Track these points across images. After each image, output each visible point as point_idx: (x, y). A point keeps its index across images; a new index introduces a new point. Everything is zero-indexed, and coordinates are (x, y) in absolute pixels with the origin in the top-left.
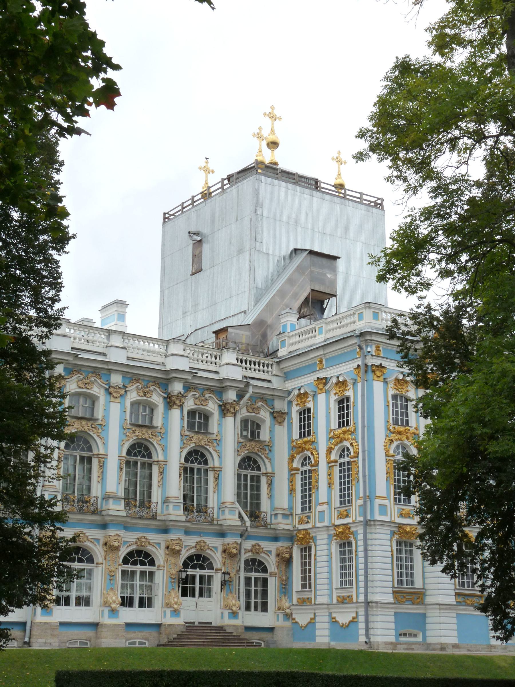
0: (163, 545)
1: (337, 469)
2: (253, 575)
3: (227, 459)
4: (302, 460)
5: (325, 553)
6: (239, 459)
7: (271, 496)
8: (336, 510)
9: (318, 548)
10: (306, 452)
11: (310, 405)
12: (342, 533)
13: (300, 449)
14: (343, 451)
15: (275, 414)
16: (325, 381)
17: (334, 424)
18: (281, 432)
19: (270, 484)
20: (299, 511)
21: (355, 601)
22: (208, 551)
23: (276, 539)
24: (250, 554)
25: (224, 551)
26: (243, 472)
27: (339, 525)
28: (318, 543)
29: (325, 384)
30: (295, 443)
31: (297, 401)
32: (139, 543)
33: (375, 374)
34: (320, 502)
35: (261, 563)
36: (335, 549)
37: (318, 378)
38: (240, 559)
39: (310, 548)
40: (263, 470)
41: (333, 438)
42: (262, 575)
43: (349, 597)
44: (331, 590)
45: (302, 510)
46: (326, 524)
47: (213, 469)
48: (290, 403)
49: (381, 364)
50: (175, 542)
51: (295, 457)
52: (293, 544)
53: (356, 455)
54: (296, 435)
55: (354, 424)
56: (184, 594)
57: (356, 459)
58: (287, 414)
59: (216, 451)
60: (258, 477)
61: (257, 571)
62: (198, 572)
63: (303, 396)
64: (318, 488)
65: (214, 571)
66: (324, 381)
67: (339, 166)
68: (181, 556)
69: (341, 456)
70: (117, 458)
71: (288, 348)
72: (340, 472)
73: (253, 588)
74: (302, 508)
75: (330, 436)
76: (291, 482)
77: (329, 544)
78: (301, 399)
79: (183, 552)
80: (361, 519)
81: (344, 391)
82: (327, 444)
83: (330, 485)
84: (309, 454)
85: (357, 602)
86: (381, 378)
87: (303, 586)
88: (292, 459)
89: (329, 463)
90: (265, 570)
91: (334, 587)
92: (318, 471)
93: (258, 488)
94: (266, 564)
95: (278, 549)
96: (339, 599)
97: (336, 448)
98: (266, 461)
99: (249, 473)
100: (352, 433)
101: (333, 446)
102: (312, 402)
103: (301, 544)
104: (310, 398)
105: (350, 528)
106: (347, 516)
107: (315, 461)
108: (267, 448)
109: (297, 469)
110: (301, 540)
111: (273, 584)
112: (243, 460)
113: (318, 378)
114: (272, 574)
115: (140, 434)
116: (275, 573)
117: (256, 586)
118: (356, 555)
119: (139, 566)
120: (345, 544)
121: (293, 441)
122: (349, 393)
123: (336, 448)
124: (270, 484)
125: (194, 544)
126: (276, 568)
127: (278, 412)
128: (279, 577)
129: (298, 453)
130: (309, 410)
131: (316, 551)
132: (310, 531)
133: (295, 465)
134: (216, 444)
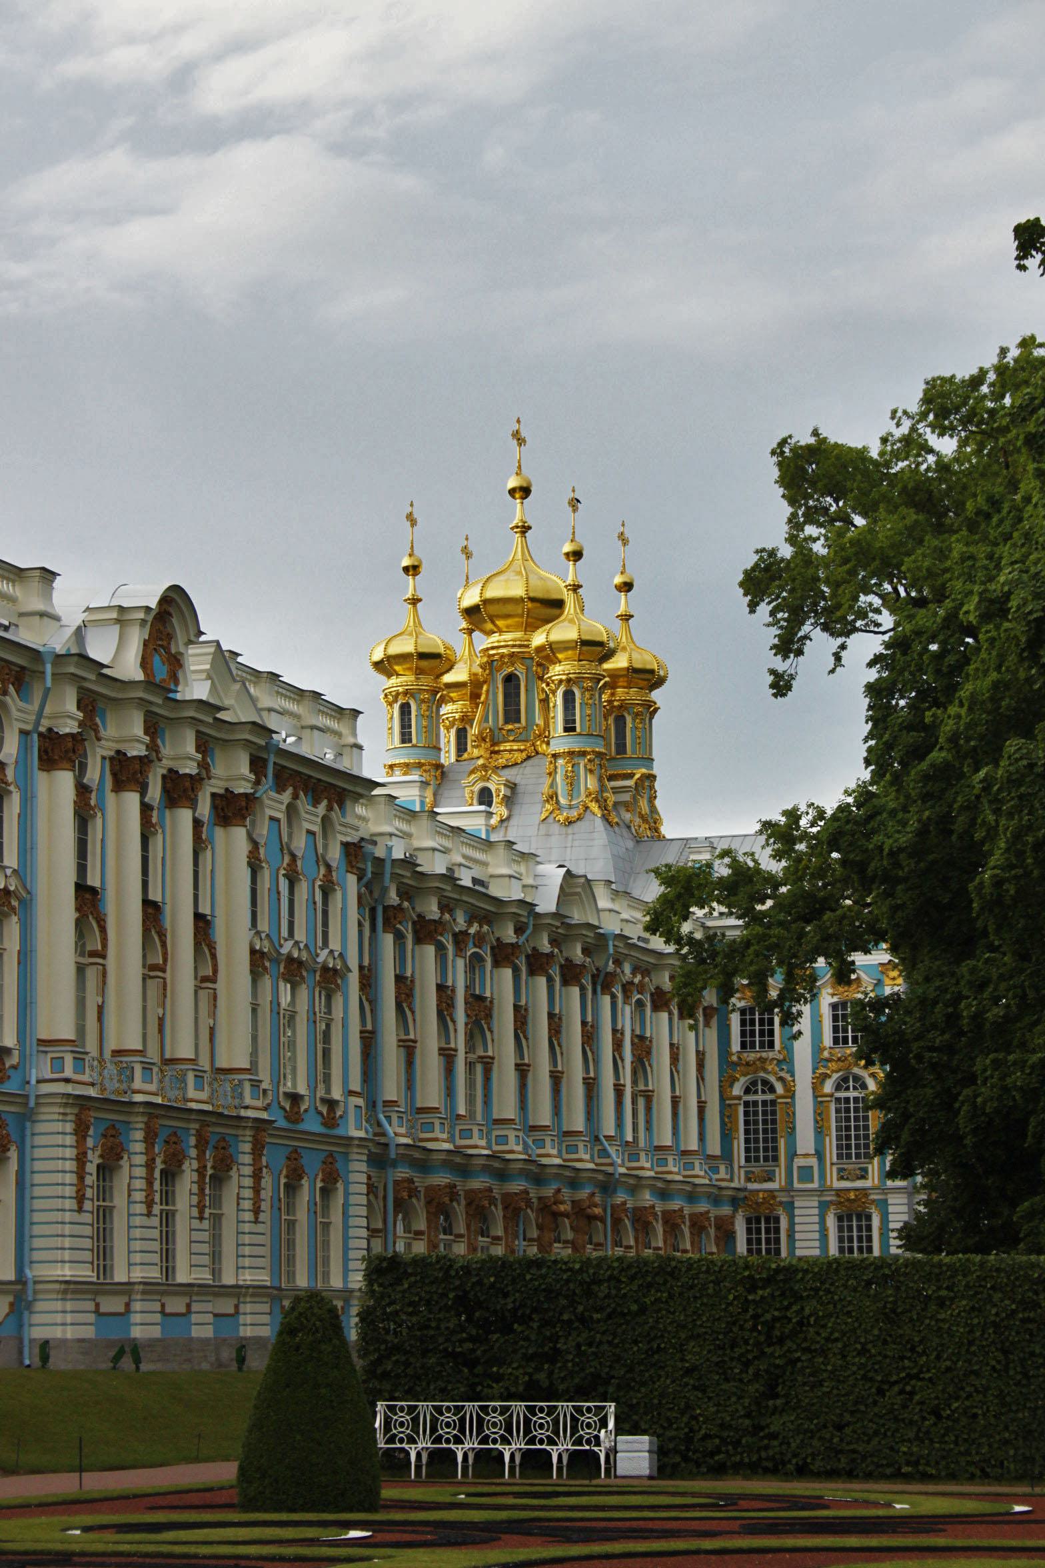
10: (762, 1074)
27: (848, 1190)
28: (797, 1212)
30: (734, 1058)
36: (831, 1222)
45: (748, 1159)
46: (815, 1185)
64: (793, 1129)
84: (772, 1079)
89: (815, 1097)
97: (835, 1076)
109: (739, 1098)
129: (745, 1075)
131: (792, 1224)
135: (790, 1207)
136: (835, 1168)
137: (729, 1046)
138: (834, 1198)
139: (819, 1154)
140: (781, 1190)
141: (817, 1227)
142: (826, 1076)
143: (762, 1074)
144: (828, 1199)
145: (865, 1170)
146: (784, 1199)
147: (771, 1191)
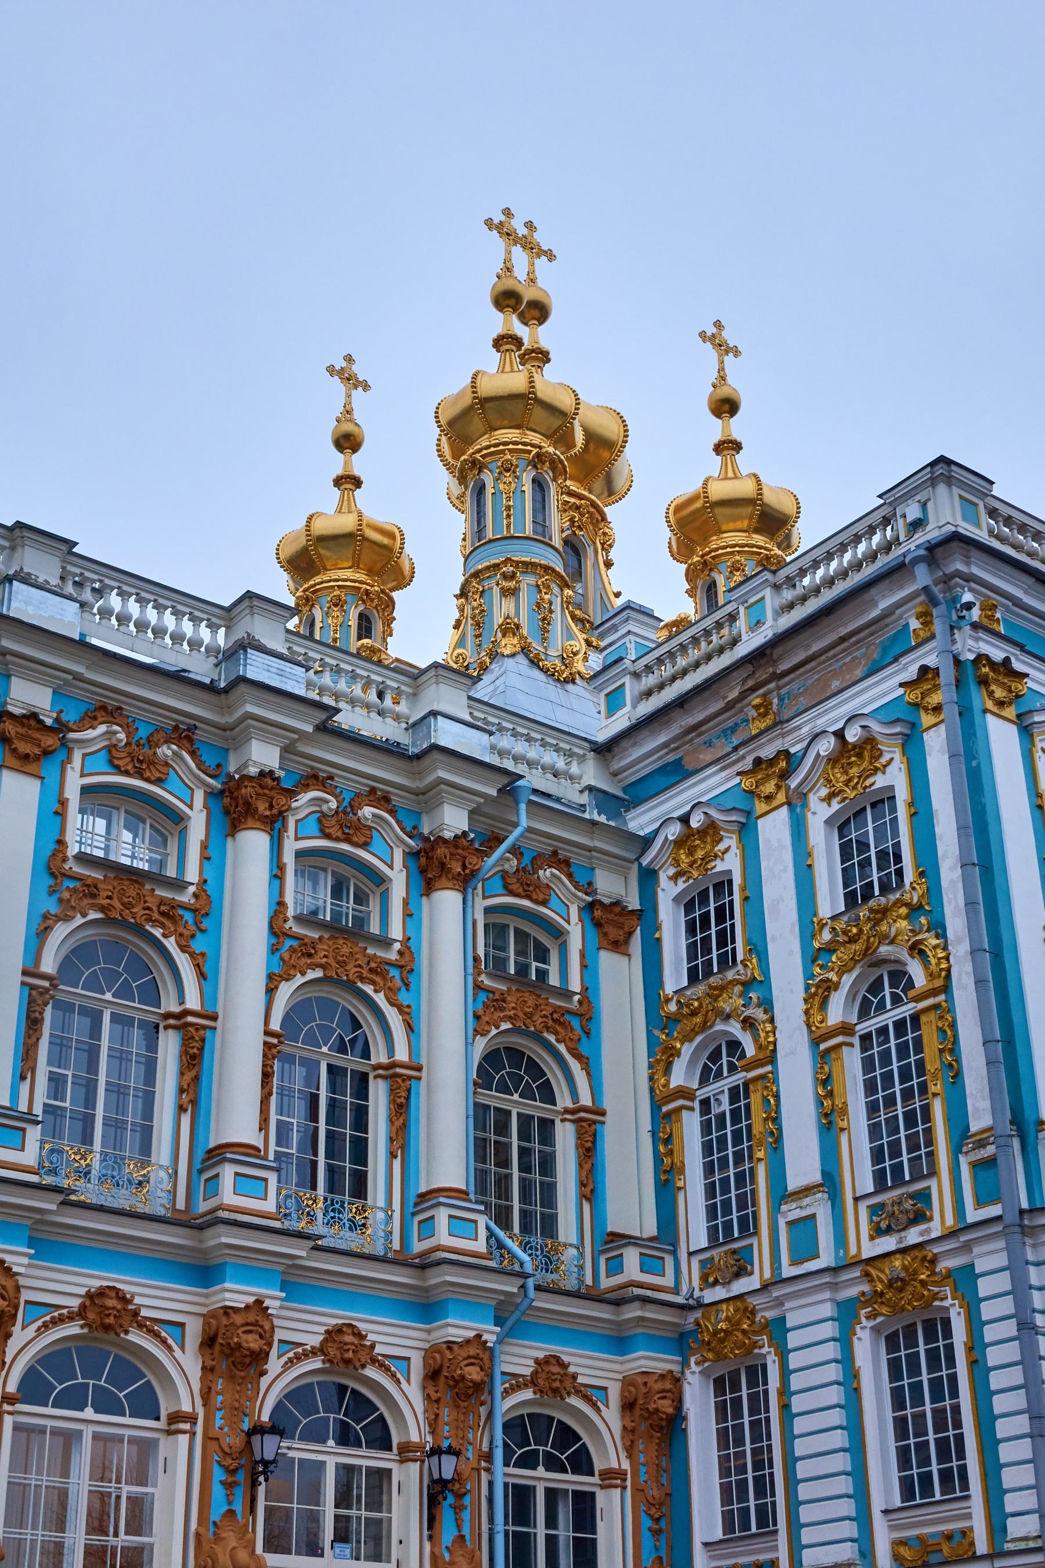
0: (194, 1330)
1: (852, 1059)
2: (541, 1478)
3: (444, 1037)
4: (704, 1059)
5: (828, 1376)
6: (481, 1045)
7: (590, 1189)
8: (863, 1207)
9: (795, 1360)
10: (719, 1027)
11: (731, 863)
12: (898, 1284)
13: (698, 1020)
14: (876, 987)
15: (598, 913)
16: (785, 764)
17: (829, 900)
18: (619, 980)
19: (588, 1149)
20: (701, 1240)
21: (982, 1547)
22: (371, 1372)
23: (619, 1342)
24: (528, 1394)
25: (432, 1375)
26: (494, 1099)
28: (793, 1339)
29: (785, 775)
30: (673, 1007)
31: (677, 862)
32: (91, 1316)
33: (991, 694)
34: (793, 1185)
35: (567, 1436)
36: (868, 1353)
37: (758, 761)
38: (490, 1415)
39: (757, 1373)
40: (564, 1101)
41: (829, 949)
42: (570, 1481)
43: (949, 1537)
44: (863, 1517)
46: (825, 1260)
47: (390, 1071)
48: (648, 877)
49: (1007, 660)
50: (238, 1319)
51: (678, 1053)
52: (685, 1364)
53: (939, 983)
54: (674, 977)
55: (922, 874)
56: (276, 1543)
57: (942, 997)
58: (638, 914)
59: (401, 1009)
60: (547, 1126)
61: (553, 1464)
62: (331, 1456)
63: (696, 839)
64: (778, 1139)
65: (394, 1455)
66: (783, 764)
67: (720, 355)
68: (264, 1382)
69: (864, 1013)
70: (19, 978)
71: (634, 707)
72: (868, 1065)
73: (541, 1531)
74: (713, 1232)
75: (817, 945)
76: (664, 1138)
77: (845, 1341)
78: (691, 852)
79: (274, 1364)
80: (995, 1210)
81: (863, 776)
82: (809, 976)
83: (830, 1120)
84: (734, 1028)
85: (995, 1554)
86: (1011, 712)
87: (734, 1522)
88: (663, 1058)
89: (816, 1042)
90: (582, 1463)
91: (877, 1505)
92: (775, 1081)
93: (548, 1165)
94: (586, 1439)
95: (627, 1382)
96: (904, 1552)
97: (848, 980)
98: (575, 1065)
99: (515, 1104)
100: (915, 909)
101: (833, 976)
102: (735, 850)
103: (720, 1357)
104: (730, 841)
105: (933, 1261)
106: (920, 1217)
107: (760, 1047)
108: (575, 1023)
110: (714, 1345)
111: (614, 1513)
112: (491, 1058)
113: (758, 761)
114: (611, 1477)
115: (116, 903)
116: (621, 1474)
117: (551, 1521)
118: (976, 1363)
119: (89, 1413)
120: (910, 1332)
121: (668, 1000)
122: (895, 777)
123: (848, 980)
124: (588, 1149)
125: (314, 1341)
126: (623, 1455)
127: (607, 908)
128: (638, 1490)
129: (687, 1038)
130: (723, 885)
131: (785, 1373)
132: (753, 1301)
133: (678, 1077)
134: (398, 982)
135: (777, 1330)
136: (863, 1207)
137: (661, 984)
138: (866, 1288)
139: (830, 1182)
140: (765, 1287)
141: (833, 1372)
142: (828, 987)
143: (719, 1027)
144: (853, 1292)
145: (924, 1196)
146: (769, 1315)
147: (740, 1297)
